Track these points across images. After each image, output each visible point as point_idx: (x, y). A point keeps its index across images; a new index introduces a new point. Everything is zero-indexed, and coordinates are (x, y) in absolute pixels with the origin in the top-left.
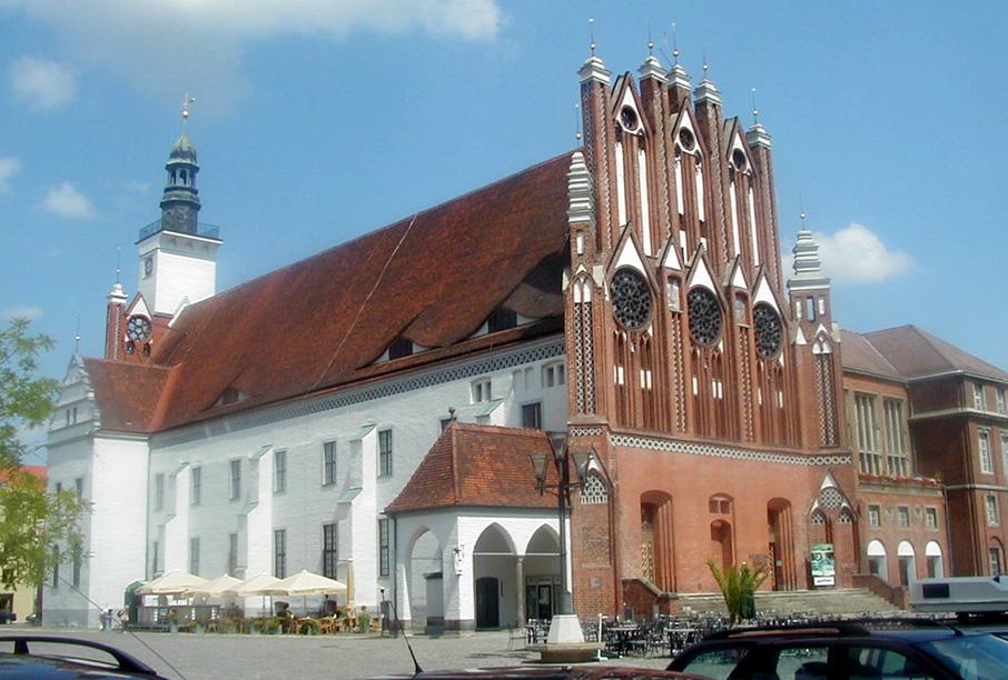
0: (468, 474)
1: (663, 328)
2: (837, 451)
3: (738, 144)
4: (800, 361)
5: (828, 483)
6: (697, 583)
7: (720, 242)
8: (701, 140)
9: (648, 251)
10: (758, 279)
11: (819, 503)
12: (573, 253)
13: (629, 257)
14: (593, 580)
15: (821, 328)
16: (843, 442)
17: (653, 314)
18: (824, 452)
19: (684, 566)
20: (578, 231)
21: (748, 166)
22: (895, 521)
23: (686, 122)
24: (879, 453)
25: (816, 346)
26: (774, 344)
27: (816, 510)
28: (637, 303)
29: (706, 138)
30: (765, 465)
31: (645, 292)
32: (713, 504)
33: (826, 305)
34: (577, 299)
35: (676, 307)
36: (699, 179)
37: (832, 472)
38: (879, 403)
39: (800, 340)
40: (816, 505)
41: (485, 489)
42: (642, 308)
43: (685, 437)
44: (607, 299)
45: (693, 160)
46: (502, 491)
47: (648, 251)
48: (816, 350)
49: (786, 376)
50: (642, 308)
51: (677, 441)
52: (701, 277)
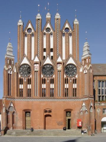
2: (86, 96)
5: (84, 104)
13: (25, 61)
15: (85, 67)
17: (32, 73)
18: (84, 97)
19: (35, 124)
21: (70, 31)
26: (75, 73)
32: (46, 111)
33: (91, 60)
36: (52, 39)
40: (81, 110)
42: (29, 71)
43: (37, 97)
44: (15, 71)
47: (32, 59)
48: (84, 73)
50: (29, 71)
51: (34, 98)
52: (48, 61)
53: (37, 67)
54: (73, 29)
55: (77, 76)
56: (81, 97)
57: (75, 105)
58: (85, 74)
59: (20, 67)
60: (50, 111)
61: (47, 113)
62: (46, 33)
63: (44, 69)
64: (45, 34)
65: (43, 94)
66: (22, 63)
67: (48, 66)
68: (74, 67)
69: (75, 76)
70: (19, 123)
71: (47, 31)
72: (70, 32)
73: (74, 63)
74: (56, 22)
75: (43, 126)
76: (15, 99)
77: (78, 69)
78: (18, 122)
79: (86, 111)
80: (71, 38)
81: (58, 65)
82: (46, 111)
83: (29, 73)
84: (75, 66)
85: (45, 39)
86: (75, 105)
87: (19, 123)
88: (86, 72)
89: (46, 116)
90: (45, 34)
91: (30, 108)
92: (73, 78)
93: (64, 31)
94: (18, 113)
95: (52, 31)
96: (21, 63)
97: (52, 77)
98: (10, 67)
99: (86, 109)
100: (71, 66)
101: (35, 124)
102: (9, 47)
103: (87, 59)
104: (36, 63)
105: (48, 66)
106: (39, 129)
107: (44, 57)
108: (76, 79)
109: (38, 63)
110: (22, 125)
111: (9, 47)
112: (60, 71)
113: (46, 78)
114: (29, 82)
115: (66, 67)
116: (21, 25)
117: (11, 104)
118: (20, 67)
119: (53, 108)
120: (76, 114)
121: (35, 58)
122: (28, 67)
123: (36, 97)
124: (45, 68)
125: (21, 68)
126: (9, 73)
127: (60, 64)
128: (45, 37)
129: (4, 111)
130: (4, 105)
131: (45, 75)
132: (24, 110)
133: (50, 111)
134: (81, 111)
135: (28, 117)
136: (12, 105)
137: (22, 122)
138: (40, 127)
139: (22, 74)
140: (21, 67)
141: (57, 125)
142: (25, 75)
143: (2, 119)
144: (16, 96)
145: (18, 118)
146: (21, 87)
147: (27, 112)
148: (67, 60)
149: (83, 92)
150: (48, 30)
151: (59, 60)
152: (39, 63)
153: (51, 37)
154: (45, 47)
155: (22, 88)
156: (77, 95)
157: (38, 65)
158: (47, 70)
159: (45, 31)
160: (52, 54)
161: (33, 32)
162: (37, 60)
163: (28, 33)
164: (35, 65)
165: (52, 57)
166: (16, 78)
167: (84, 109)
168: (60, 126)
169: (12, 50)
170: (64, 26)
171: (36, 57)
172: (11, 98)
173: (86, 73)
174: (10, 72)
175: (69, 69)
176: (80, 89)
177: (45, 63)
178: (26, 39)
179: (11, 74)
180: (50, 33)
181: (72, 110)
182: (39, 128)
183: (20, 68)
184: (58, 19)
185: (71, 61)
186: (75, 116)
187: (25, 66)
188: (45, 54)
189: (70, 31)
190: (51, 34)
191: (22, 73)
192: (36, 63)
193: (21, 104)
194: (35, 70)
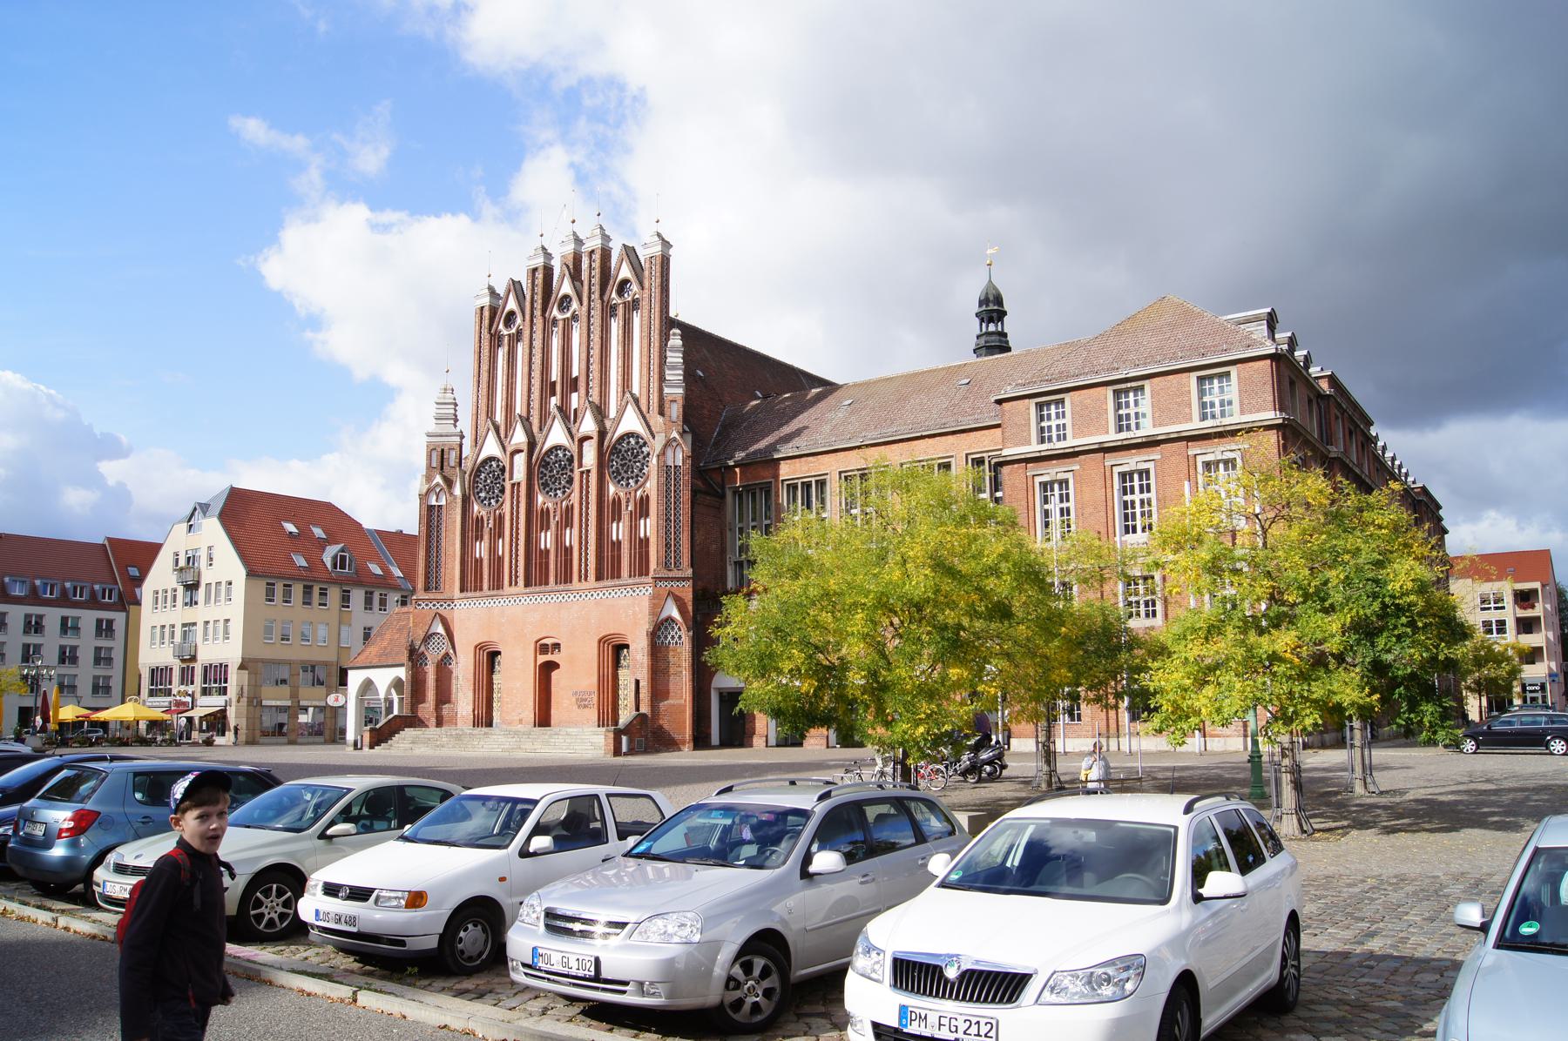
13: (491, 448)
44: (457, 491)
52: (557, 435)
59: (479, 471)
63: (549, 469)
65: (537, 572)
70: (464, 701)
75: (528, 712)
82: (544, 649)
87: (464, 701)
90: (555, 322)
91: (494, 638)
92: (639, 493)
95: (575, 305)
98: (438, 479)
115: (614, 447)
126: (434, 503)
132: (480, 647)
133: (557, 646)
136: (440, 629)
137: (471, 694)
152: (525, 448)
172: (438, 601)
182: (521, 721)
185: (631, 422)
190: (575, 317)
191: (483, 495)
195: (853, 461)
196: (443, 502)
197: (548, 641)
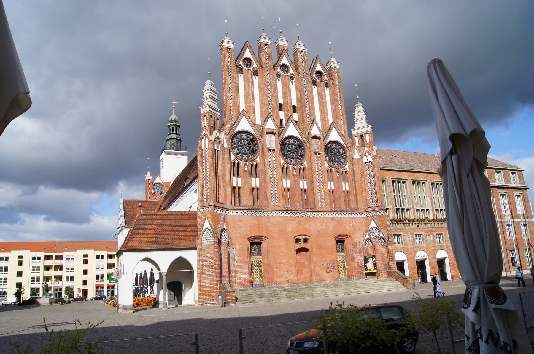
0: (138, 234)
1: (263, 158)
2: (377, 208)
3: (319, 68)
4: (356, 167)
5: (373, 224)
6: (286, 280)
7: (304, 114)
8: (293, 68)
9: (258, 121)
10: (330, 129)
11: (369, 235)
12: (203, 126)
13: (244, 125)
14: (207, 282)
15: (366, 149)
16: (380, 204)
17: (260, 152)
19: (277, 272)
20: (205, 116)
21: (326, 77)
22: (434, 240)
23: (284, 61)
24: (430, 208)
25: (365, 158)
26: (342, 160)
27: (367, 240)
28: (250, 147)
29: (296, 68)
30: (332, 219)
31: (255, 141)
32: (297, 241)
34: (203, 148)
35: (274, 146)
37: (375, 219)
38: (428, 184)
39: (356, 156)
40: (367, 236)
41: (144, 240)
42: (253, 149)
43: (279, 208)
44: (226, 145)
45: (288, 78)
46: (156, 242)
47: (258, 121)
48: (365, 160)
49: (349, 175)
50: (253, 149)
52: (292, 131)
53: (271, 142)
54: (330, 75)
55: (347, 167)
56: (363, 210)
57: (353, 225)
58: (366, 163)
59: (234, 137)
60: (305, 240)
61: (302, 245)
62: (282, 74)
64: (278, 75)
66: (238, 129)
67: (292, 141)
68: (340, 149)
69: (344, 167)
71: (282, 70)
72: (326, 80)
73: (341, 141)
74: (299, 55)
76: (229, 211)
77: (348, 154)
78: (238, 268)
79: (382, 238)
80: (327, 92)
81: (314, 140)
83: (254, 152)
84: (343, 147)
85: (279, 85)
86: (353, 225)
87: (241, 273)
88: (370, 159)
89: (299, 251)
90: (278, 75)
93: (314, 76)
94: (238, 247)
95: (291, 71)
96: (236, 127)
97: (302, 164)
98: (218, 135)
99: (381, 235)
100: (334, 146)
101: (277, 272)
102: (211, 90)
103: (367, 136)
104: (270, 133)
105: (292, 141)
106: (287, 284)
107: (281, 120)
108: (346, 172)
109: (275, 131)
110: (247, 276)
111: (211, 90)
112: (319, 154)
113: (290, 166)
114: (254, 171)
115: (326, 146)
116: (229, 49)
117: (223, 225)
118: (234, 137)
119: (313, 233)
120: (358, 246)
121: (265, 121)
122: (251, 140)
123: (276, 208)
124: (286, 144)
125: (235, 140)
127: (317, 140)
128: (280, 82)
129: (207, 240)
130: (207, 225)
131: (287, 158)
132: (249, 239)
133: (305, 240)
134: (368, 239)
135: (255, 257)
138: (288, 279)
139: (237, 154)
140: (236, 137)
141: (324, 272)
142: (245, 156)
143: (199, 262)
144: (229, 205)
145: (237, 257)
146: (237, 182)
147: (255, 244)
148: (327, 133)
149: (365, 200)
150: (285, 67)
151: (315, 131)
152: (277, 132)
153: (291, 84)
154: (281, 101)
155: (240, 185)
156: (353, 206)
157: (273, 136)
158: (292, 149)
159: (279, 70)
160: (296, 117)
161: (255, 68)
162: (270, 125)
163: (245, 68)
164: (268, 136)
165: (296, 122)
166: (227, 161)
167: (375, 234)
168: (331, 274)
169: (216, 97)
170: (314, 67)
171: (270, 120)
173: (370, 162)
174: (217, 147)
175: (332, 152)
176: (358, 192)
177: (287, 134)
178: (241, 78)
179: (218, 151)
180: (288, 75)
181: (347, 236)
182: (288, 282)
183: (232, 139)
184: (302, 52)
185: (334, 136)
186: (356, 251)
187: (244, 136)
188: (282, 115)
189: (326, 77)
190: (291, 78)
191: (236, 150)
192: (270, 133)
193: (241, 224)
194: (268, 146)
195: (397, 176)
196: (219, 149)
197: (302, 237)
